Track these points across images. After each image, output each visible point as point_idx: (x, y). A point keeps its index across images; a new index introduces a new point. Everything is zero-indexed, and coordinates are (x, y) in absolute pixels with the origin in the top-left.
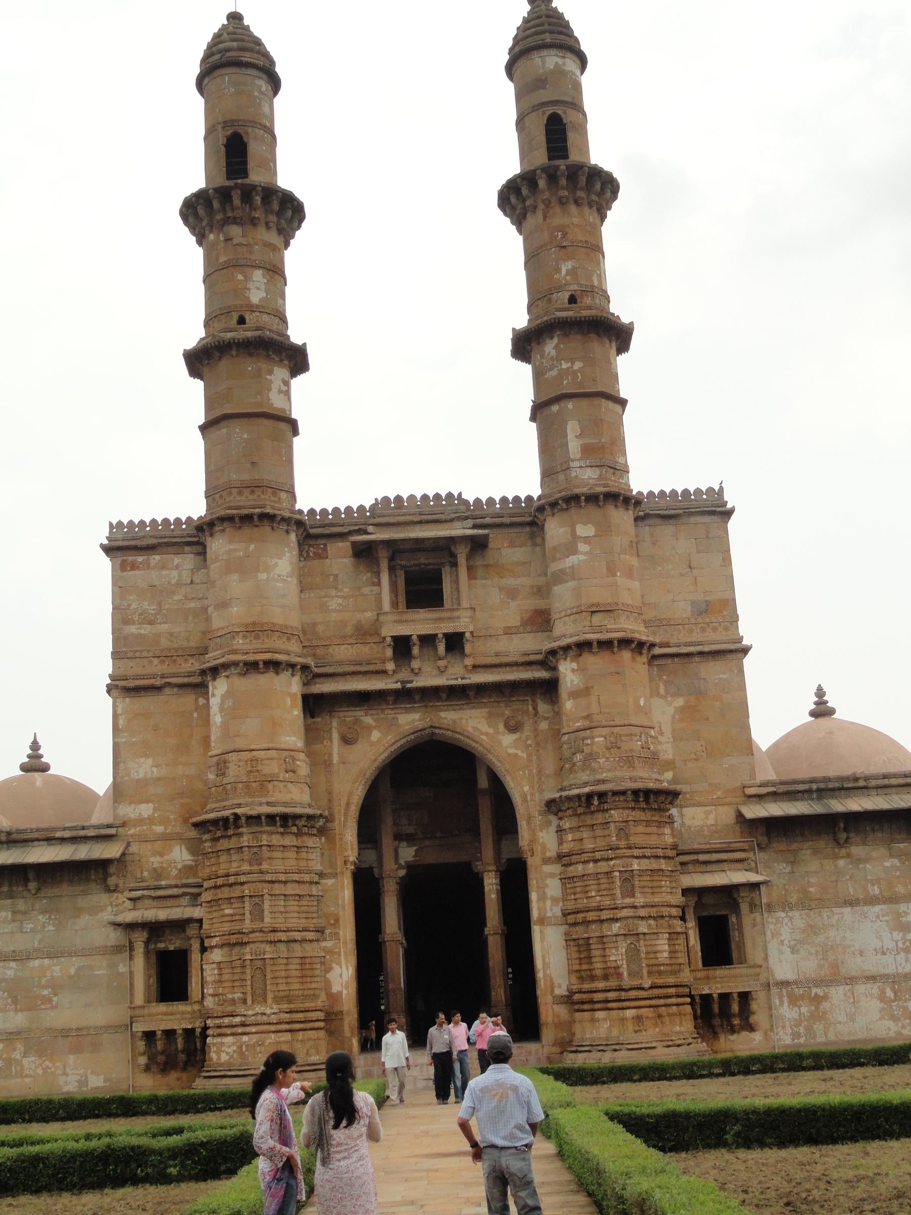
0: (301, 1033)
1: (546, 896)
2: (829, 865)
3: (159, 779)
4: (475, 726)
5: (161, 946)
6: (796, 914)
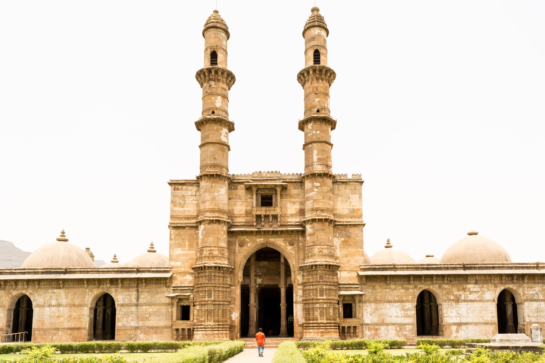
1: (298, 295)
2: (384, 291)
4: (279, 243)
5: (182, 304)
6: (372, 304)
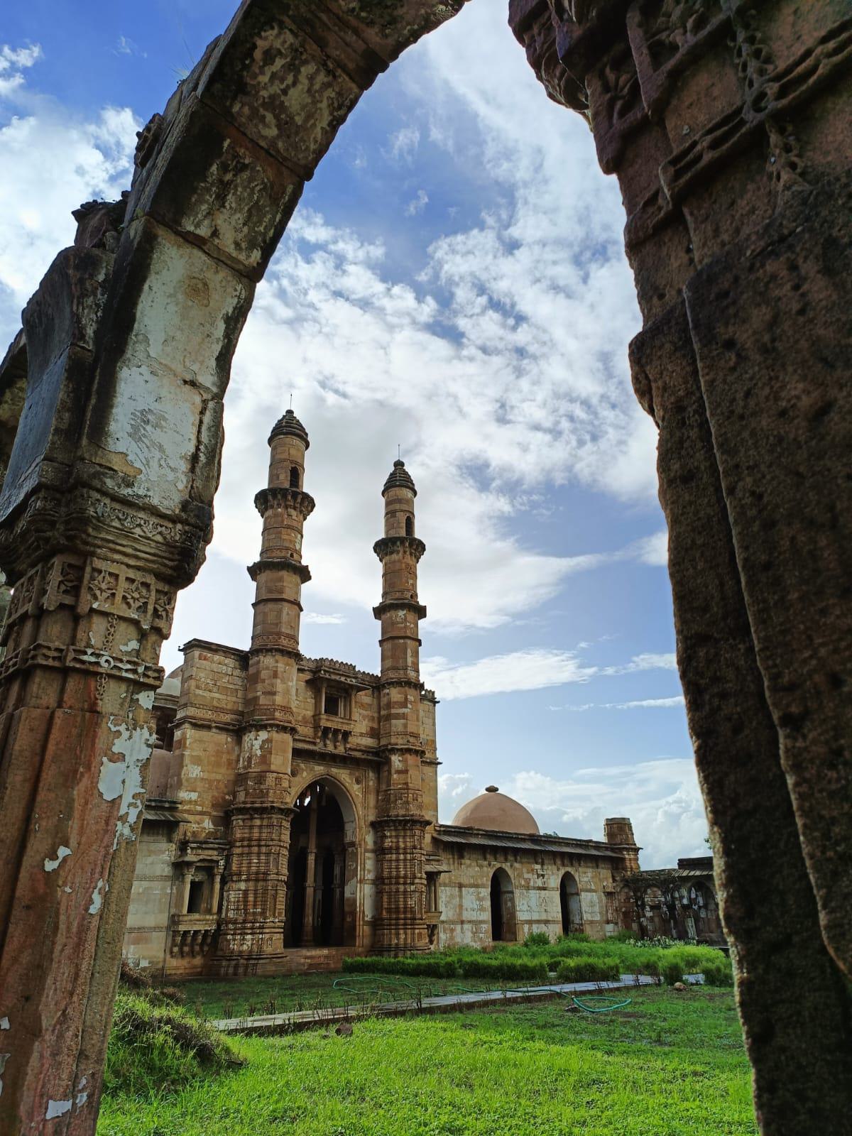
3: (202, 779)
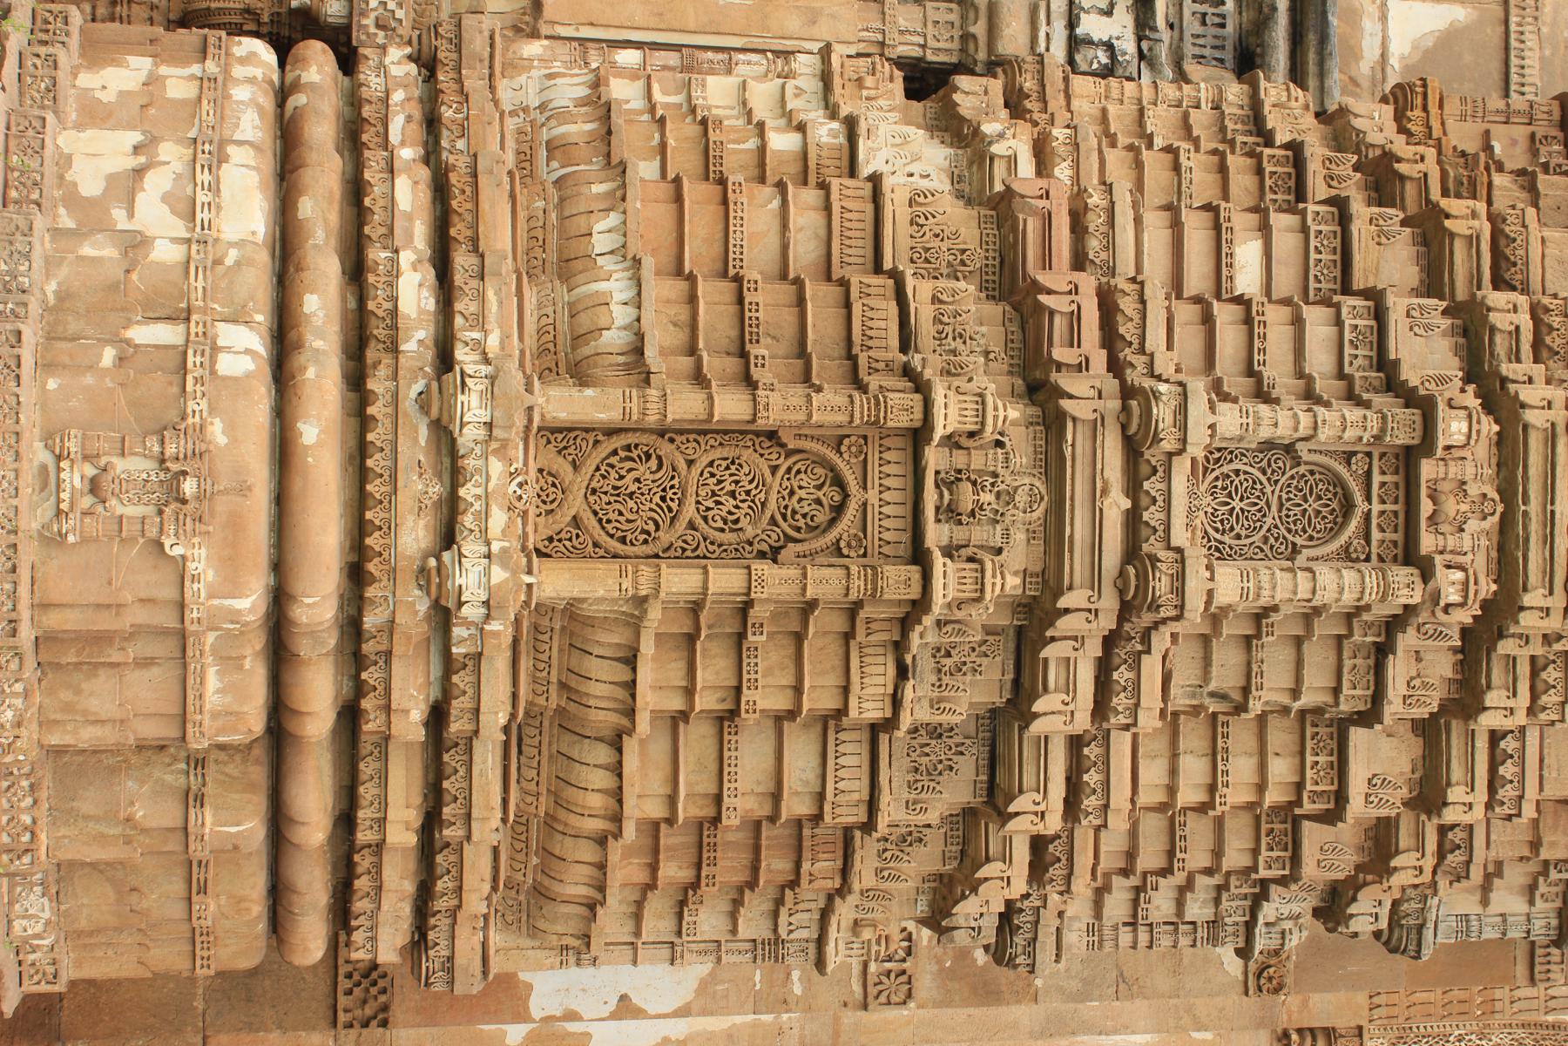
0: (251, 828)
